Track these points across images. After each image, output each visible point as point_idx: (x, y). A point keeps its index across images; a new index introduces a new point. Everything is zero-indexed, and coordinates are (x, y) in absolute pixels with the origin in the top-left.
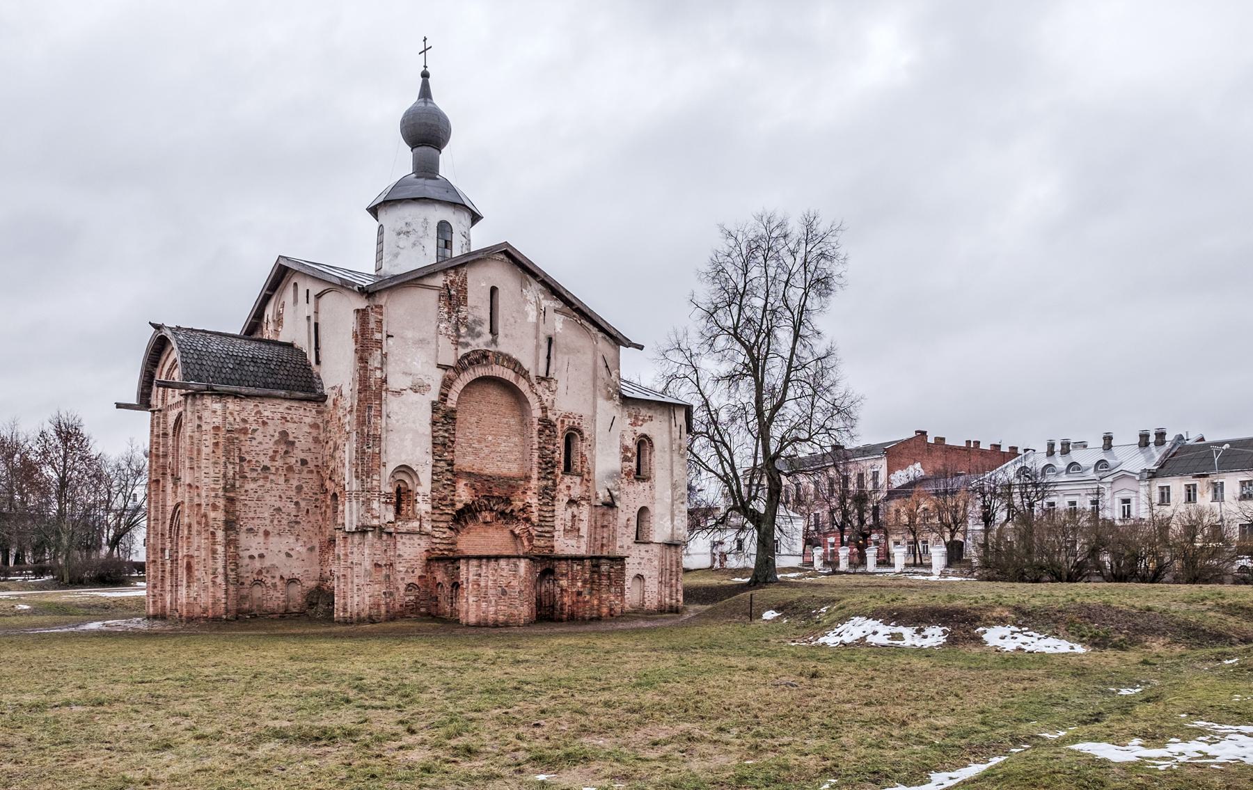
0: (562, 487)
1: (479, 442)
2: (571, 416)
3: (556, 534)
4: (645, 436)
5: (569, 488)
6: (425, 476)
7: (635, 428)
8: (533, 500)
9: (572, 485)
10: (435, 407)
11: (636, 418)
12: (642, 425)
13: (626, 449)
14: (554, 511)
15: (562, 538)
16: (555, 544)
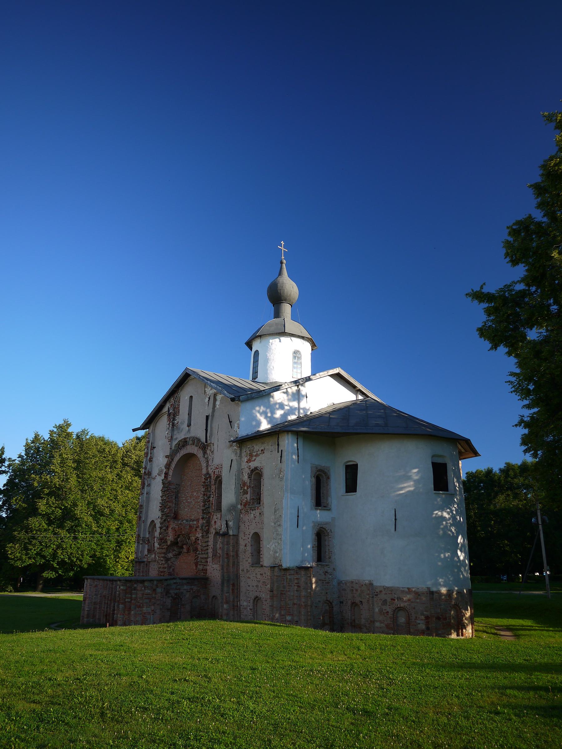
0: (213, 523)
1: (191, 497)
2: (218, 468)
3: (209, 560)
4: (256, 468)
5: (215, 522)
6: (158, 525)
7: (250, 464)
8: (199, 535)
9: (217, 520)
10: (163, 483)
11: (251, 455)
12: (255, 459)
13: (244, 484)
14: (208, 541)
15: (211, 564)
16: (208, 568)
